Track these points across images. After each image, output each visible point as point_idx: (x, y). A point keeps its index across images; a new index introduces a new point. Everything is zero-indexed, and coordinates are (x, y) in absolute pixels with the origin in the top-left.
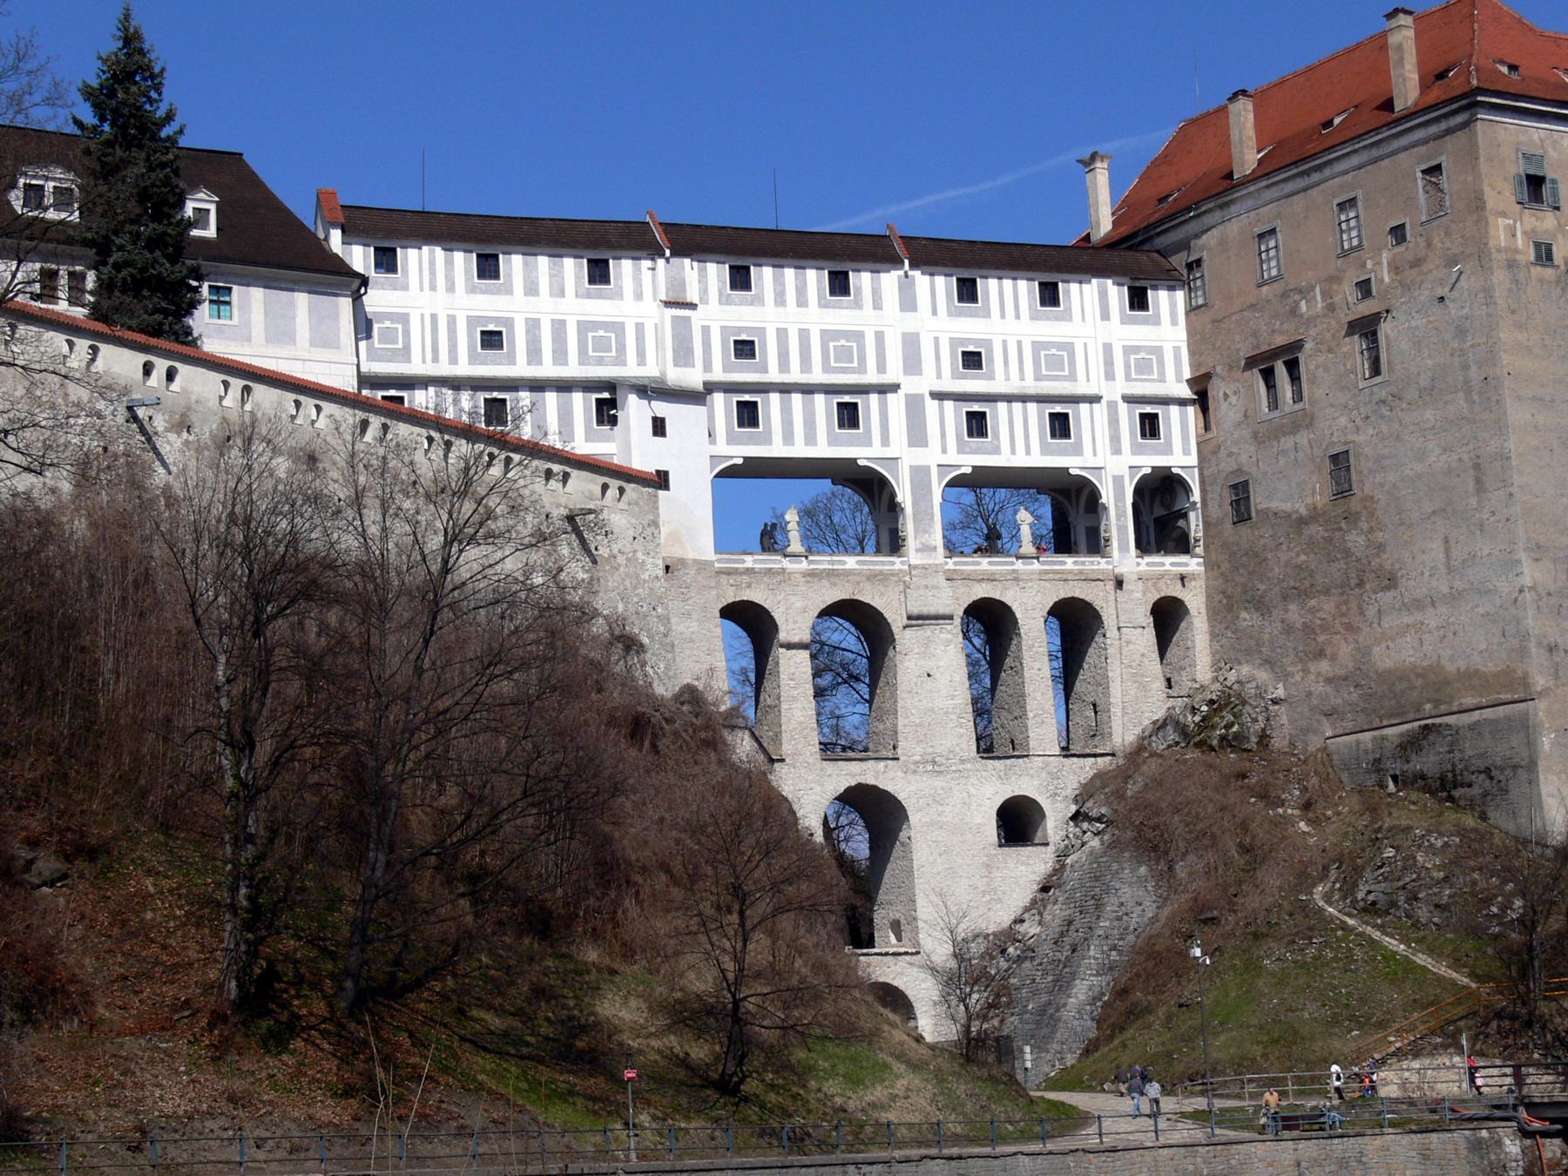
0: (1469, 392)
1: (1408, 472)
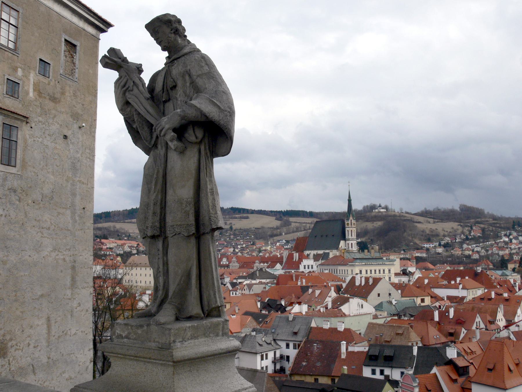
0: (73, 213)
1: (27, 257)
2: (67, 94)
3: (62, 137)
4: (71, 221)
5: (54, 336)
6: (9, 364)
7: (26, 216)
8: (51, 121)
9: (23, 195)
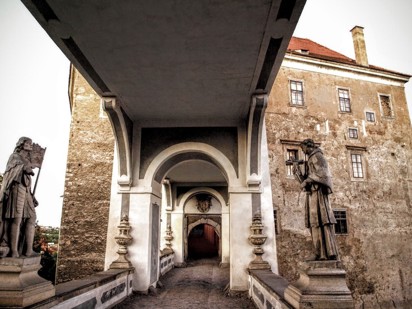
1: (379, 231)
2: (389, 128)
3: (390, 155)
4: (407, 207)
5: (406, 283)
6: (377, 298)
7: (375, 206)
8: (381, 146)
9: (370, 194)
